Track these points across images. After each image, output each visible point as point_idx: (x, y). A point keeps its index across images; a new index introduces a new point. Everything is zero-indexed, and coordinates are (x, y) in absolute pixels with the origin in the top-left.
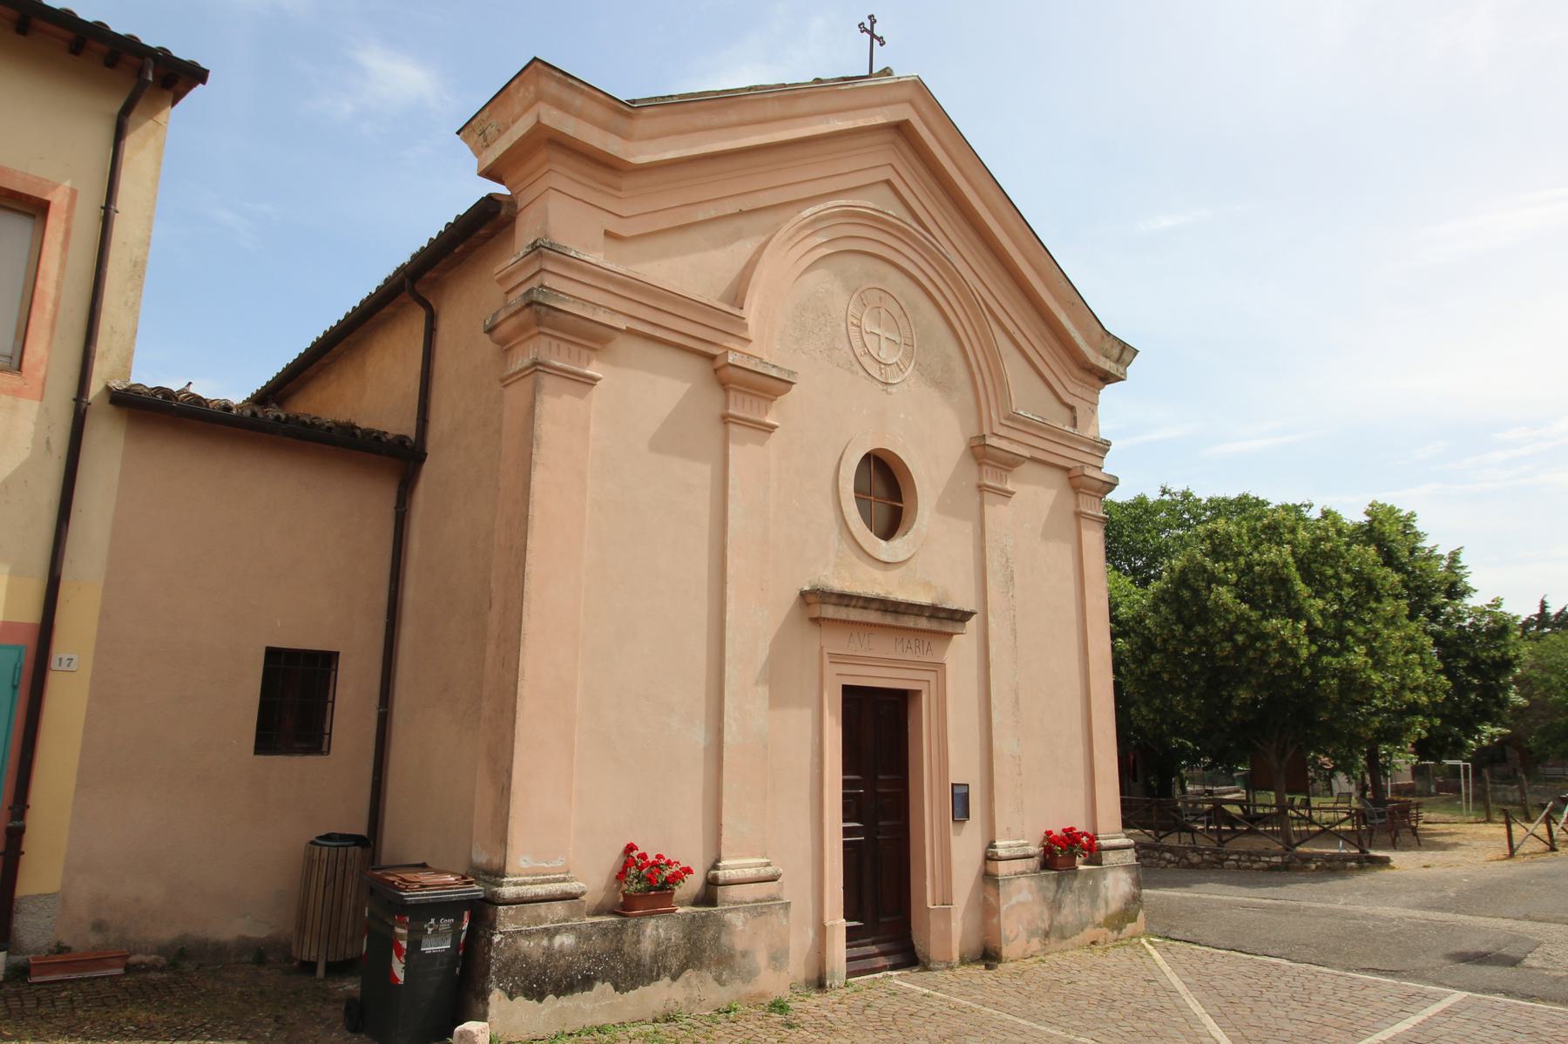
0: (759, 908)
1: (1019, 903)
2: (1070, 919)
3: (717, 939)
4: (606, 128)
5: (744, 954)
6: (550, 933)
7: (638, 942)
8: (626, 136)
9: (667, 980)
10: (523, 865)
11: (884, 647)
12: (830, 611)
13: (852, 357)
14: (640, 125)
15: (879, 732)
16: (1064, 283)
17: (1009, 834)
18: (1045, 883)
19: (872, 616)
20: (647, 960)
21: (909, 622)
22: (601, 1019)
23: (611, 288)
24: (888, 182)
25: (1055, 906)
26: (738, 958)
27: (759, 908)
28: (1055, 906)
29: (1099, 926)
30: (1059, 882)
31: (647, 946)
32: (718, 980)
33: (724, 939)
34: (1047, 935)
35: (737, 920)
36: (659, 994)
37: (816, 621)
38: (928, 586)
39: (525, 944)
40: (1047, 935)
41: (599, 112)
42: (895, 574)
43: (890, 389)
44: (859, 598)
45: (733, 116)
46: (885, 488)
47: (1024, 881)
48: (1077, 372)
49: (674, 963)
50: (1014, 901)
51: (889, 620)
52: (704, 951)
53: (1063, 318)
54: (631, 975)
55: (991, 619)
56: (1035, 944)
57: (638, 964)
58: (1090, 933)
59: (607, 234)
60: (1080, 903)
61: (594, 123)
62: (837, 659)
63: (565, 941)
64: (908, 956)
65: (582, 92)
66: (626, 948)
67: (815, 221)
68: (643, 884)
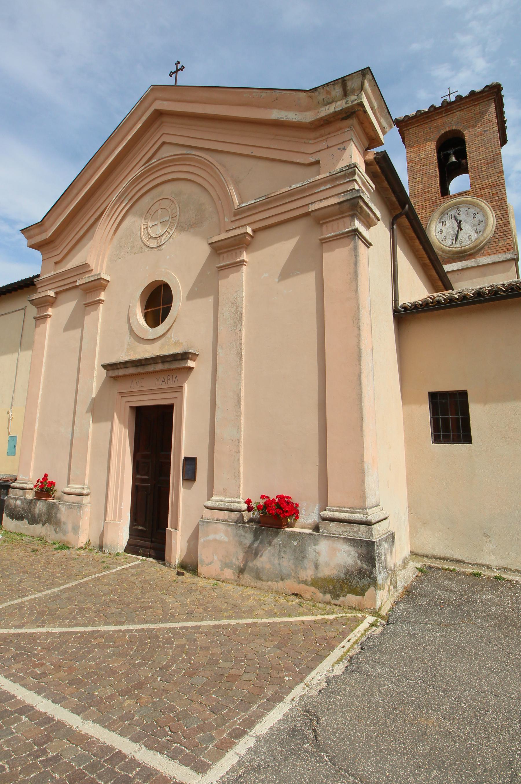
0: (71, 506)
1: (215, 540)
2: (268, 566)
3: (56, 514)
4: (41, 233)
5: (64, 523)
6: (16, 499)
7: (35, 508)
8: (46, 231)
9: (41, 525)
10: (21, 477)
11: (149, 384)
12: (121, 372)
13: (143, 245)
14: (47, 224)
15: (153, 430)
16: (264, 94)
17: (225, 492)
18: (241, 532)
19: (131, 371)
20: (37, 515)
21: (151, 368)
22: (23, 532)
23: (52, 282)
24: (164, 143)
25: (252, 553)
26: (62, 524)
27: (71, 506)
28: (252, 553)
29: (305, 582)
30: (256, 534)
31: (37, 511)
32: (55, 530)
33: (58, 515)
34: (241, 571)
35: (63, 508)
36: (39, 529)
37: (115, 378)
38: (177, 343)
39: (11, 501)
40: (241, 571)
41: (37, 231)
42: (158, 344)
43: (162, 248)
44: (119, 363)
45: (75, 191)
46: (157, 301)
47: (221, 527)
48: (312, 135)
49: (44, 519)
50: (211, 537)
51: (140, 370)
52: (52, 518)
53: (275, 115)
54: (34, 520)
55: (220, 351)
56: (229, 574)
57: (34, 517)
58: (291, 585)
59: (56, 263)
60: (280, 557)
61: (38, 234)
62: (123, 395)
63: (19, 502)
64: (159, 553)
65: (31, 229)
66: (32, 510)
67: (120, 198)
68: (45, 489)
